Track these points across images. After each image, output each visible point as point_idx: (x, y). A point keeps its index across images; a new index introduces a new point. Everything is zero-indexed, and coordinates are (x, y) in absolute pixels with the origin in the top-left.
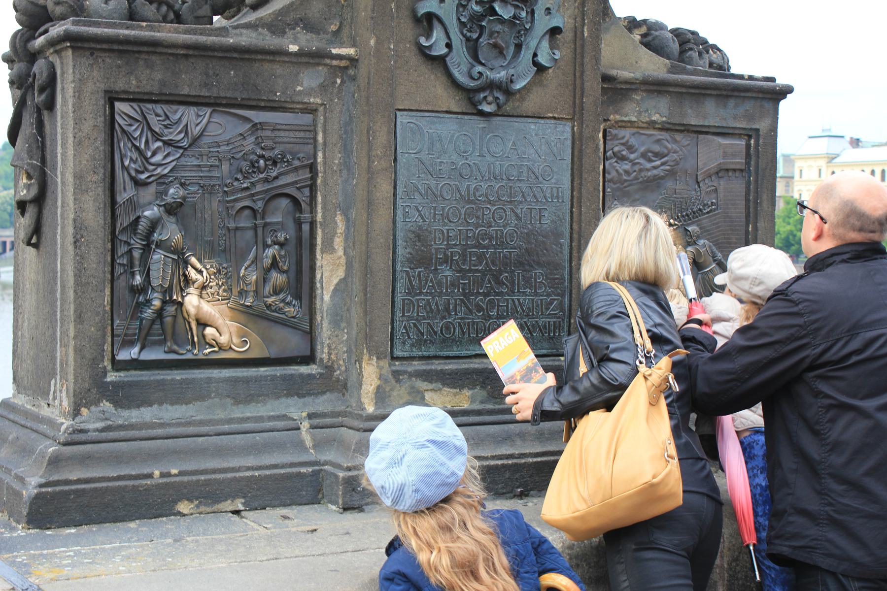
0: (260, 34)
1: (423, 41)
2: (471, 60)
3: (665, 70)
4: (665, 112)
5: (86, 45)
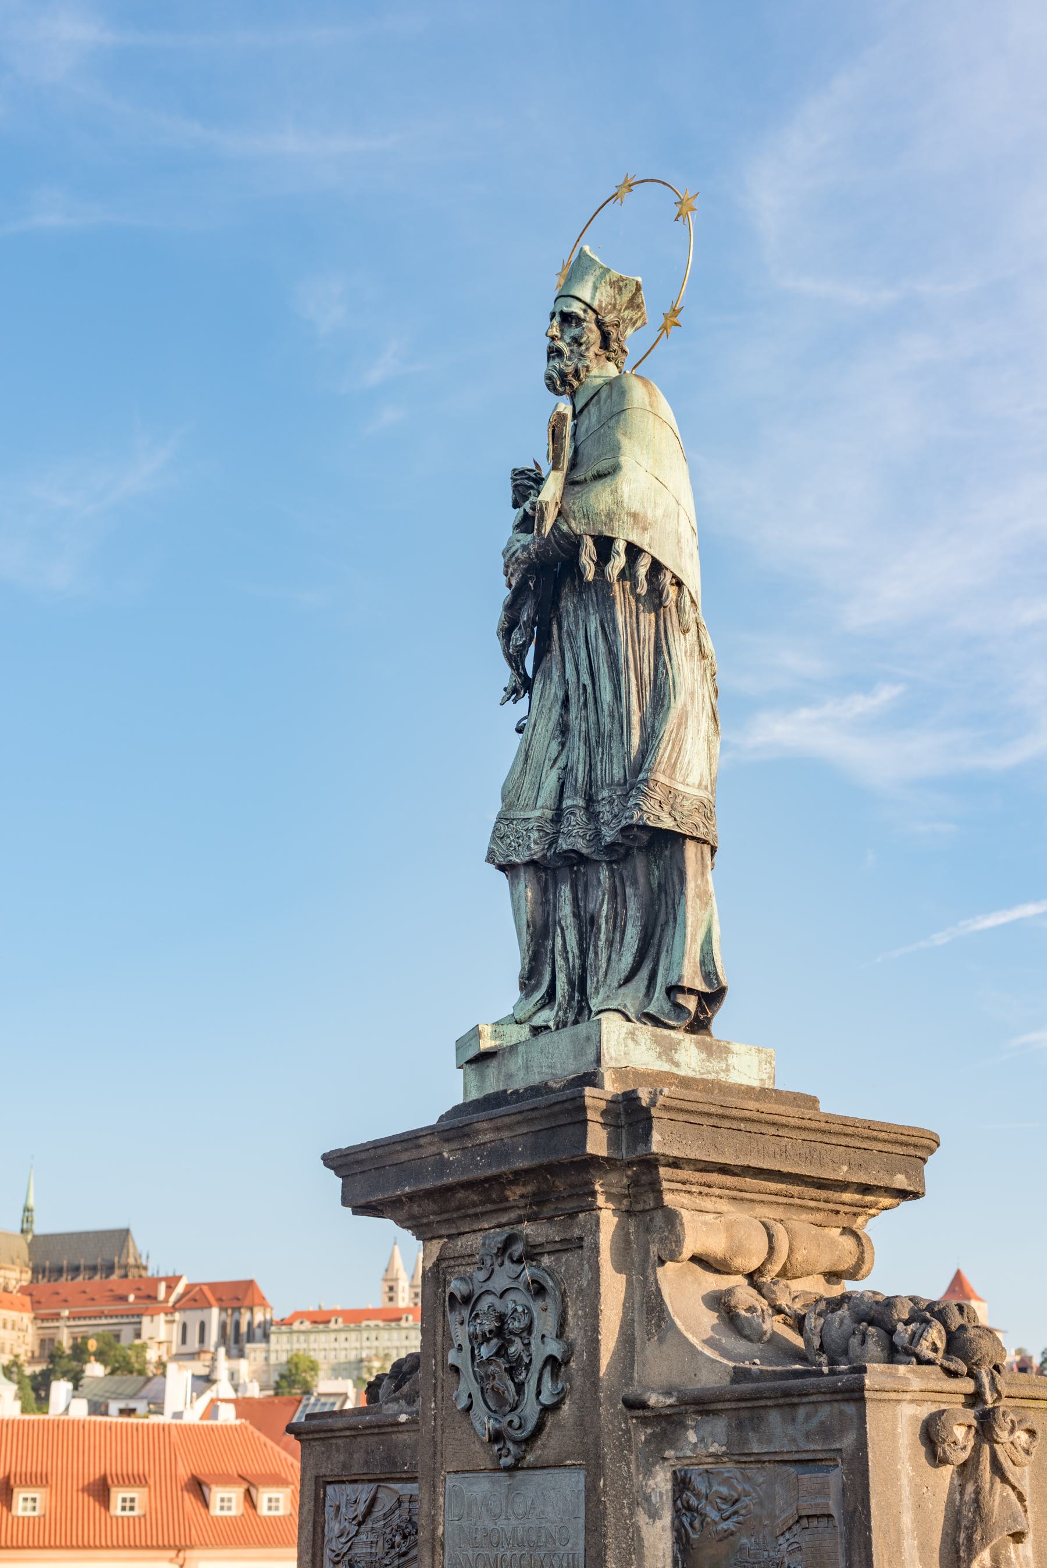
3: (728, 1379)
4: (724, 1439)
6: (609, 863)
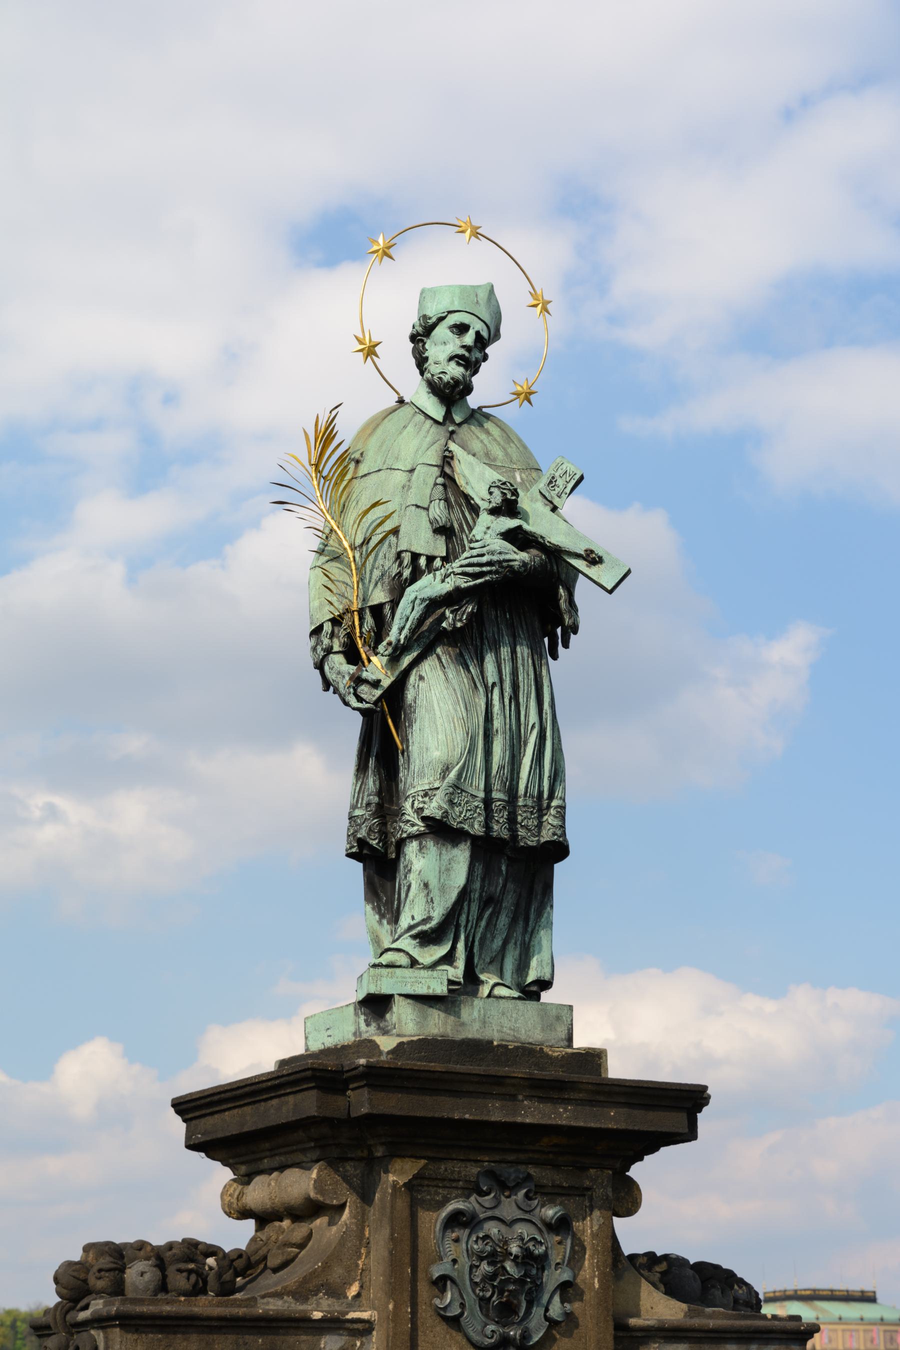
0: (286, 1302)
1: (437, 1301)
2: (484, 1319)
3: (683, 1314)
5: (133, 1322)
6: (509, 858)
